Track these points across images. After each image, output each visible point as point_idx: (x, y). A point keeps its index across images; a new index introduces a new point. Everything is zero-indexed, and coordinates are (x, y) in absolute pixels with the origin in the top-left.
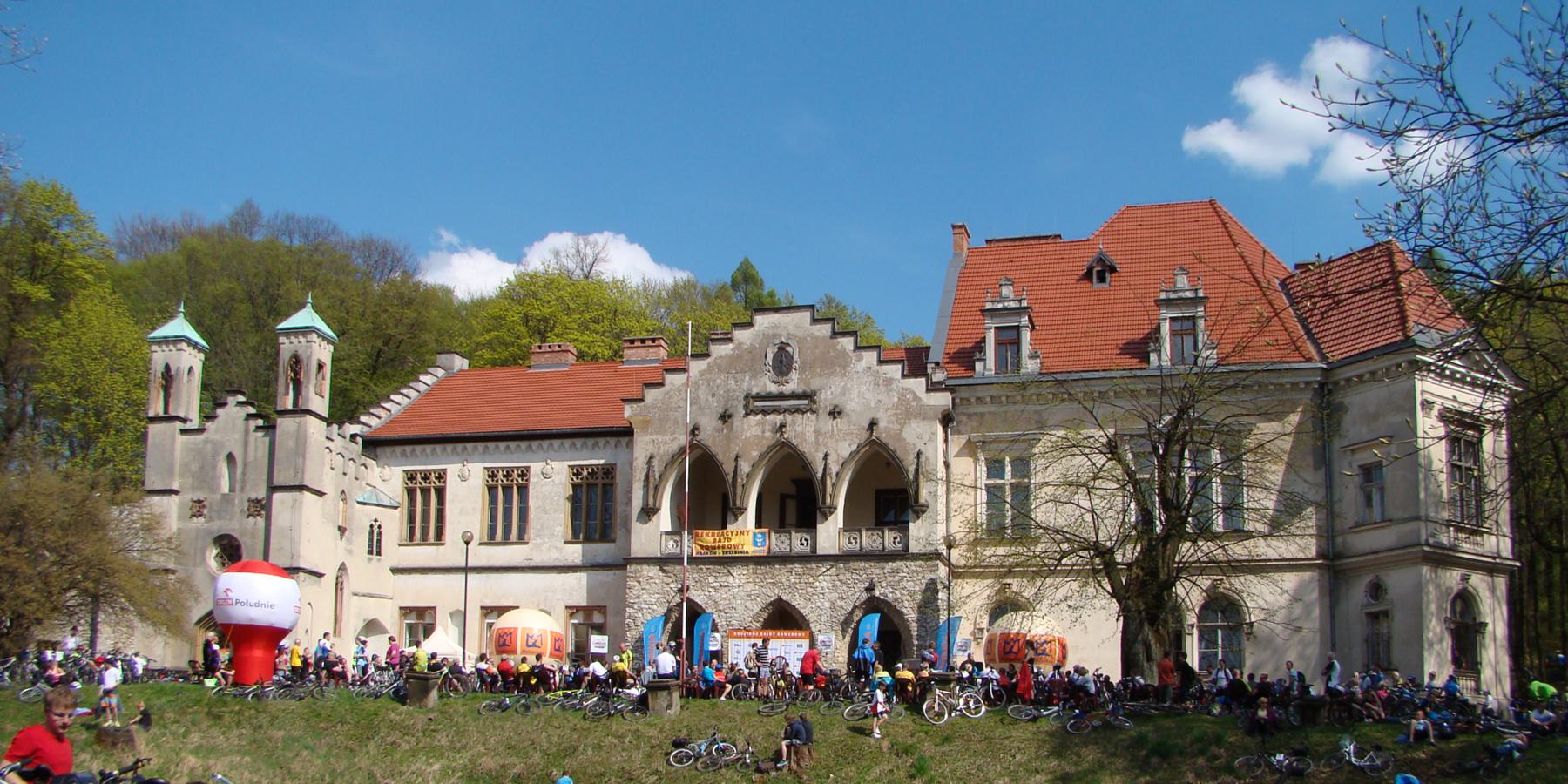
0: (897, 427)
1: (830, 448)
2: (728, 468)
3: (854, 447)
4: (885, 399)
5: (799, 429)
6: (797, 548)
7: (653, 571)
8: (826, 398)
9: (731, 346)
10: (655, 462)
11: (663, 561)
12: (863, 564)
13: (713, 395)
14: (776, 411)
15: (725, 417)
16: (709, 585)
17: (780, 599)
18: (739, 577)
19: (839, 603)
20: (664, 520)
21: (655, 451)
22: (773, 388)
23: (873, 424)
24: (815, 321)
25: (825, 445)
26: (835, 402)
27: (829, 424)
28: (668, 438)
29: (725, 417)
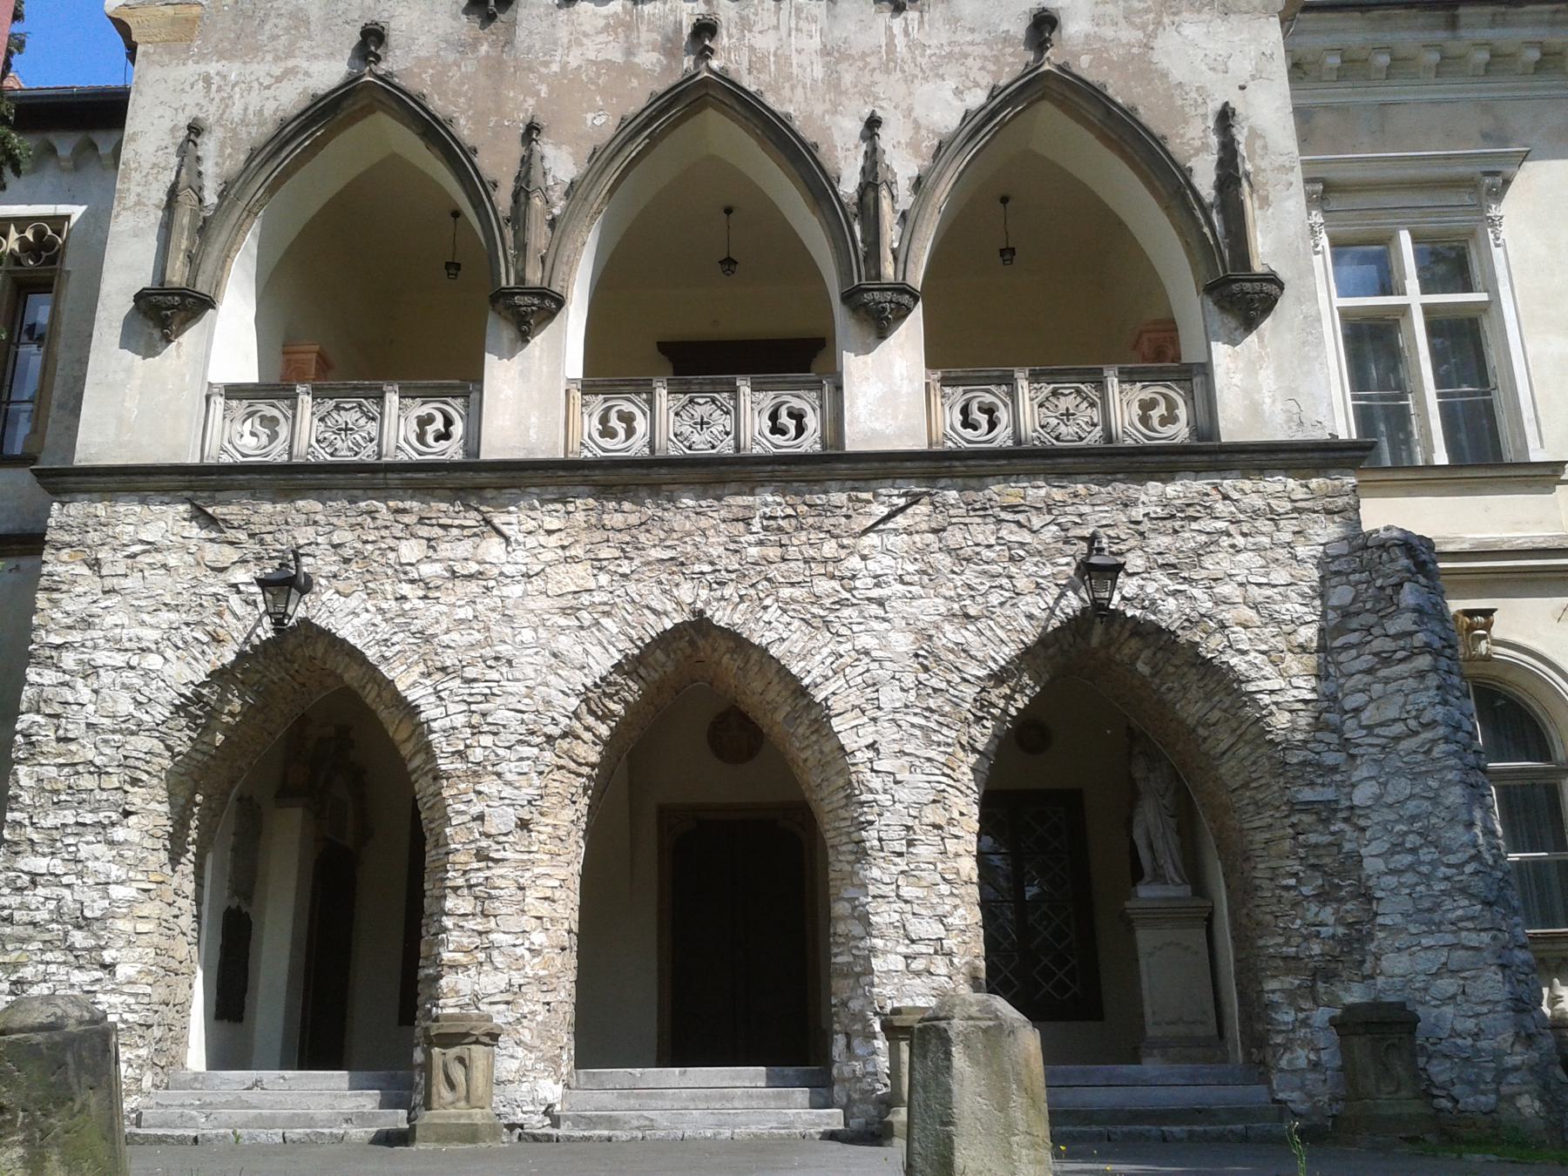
0: (1128, 35)
2: (497, 164)
3: (977, 98)
5: (765, 43)
6: (757, 436)
7: (165, 521)
10: (209, 147)
11: (200, 485)
12: (1038, 492)
16: (402, 571)
17: (700, 625)
18: (531, 533)
19: (952, 634)
20: (231, 340)
21: (210, 114)
23: (1043, 26)
25: (867, 93)
28: (262, 69)
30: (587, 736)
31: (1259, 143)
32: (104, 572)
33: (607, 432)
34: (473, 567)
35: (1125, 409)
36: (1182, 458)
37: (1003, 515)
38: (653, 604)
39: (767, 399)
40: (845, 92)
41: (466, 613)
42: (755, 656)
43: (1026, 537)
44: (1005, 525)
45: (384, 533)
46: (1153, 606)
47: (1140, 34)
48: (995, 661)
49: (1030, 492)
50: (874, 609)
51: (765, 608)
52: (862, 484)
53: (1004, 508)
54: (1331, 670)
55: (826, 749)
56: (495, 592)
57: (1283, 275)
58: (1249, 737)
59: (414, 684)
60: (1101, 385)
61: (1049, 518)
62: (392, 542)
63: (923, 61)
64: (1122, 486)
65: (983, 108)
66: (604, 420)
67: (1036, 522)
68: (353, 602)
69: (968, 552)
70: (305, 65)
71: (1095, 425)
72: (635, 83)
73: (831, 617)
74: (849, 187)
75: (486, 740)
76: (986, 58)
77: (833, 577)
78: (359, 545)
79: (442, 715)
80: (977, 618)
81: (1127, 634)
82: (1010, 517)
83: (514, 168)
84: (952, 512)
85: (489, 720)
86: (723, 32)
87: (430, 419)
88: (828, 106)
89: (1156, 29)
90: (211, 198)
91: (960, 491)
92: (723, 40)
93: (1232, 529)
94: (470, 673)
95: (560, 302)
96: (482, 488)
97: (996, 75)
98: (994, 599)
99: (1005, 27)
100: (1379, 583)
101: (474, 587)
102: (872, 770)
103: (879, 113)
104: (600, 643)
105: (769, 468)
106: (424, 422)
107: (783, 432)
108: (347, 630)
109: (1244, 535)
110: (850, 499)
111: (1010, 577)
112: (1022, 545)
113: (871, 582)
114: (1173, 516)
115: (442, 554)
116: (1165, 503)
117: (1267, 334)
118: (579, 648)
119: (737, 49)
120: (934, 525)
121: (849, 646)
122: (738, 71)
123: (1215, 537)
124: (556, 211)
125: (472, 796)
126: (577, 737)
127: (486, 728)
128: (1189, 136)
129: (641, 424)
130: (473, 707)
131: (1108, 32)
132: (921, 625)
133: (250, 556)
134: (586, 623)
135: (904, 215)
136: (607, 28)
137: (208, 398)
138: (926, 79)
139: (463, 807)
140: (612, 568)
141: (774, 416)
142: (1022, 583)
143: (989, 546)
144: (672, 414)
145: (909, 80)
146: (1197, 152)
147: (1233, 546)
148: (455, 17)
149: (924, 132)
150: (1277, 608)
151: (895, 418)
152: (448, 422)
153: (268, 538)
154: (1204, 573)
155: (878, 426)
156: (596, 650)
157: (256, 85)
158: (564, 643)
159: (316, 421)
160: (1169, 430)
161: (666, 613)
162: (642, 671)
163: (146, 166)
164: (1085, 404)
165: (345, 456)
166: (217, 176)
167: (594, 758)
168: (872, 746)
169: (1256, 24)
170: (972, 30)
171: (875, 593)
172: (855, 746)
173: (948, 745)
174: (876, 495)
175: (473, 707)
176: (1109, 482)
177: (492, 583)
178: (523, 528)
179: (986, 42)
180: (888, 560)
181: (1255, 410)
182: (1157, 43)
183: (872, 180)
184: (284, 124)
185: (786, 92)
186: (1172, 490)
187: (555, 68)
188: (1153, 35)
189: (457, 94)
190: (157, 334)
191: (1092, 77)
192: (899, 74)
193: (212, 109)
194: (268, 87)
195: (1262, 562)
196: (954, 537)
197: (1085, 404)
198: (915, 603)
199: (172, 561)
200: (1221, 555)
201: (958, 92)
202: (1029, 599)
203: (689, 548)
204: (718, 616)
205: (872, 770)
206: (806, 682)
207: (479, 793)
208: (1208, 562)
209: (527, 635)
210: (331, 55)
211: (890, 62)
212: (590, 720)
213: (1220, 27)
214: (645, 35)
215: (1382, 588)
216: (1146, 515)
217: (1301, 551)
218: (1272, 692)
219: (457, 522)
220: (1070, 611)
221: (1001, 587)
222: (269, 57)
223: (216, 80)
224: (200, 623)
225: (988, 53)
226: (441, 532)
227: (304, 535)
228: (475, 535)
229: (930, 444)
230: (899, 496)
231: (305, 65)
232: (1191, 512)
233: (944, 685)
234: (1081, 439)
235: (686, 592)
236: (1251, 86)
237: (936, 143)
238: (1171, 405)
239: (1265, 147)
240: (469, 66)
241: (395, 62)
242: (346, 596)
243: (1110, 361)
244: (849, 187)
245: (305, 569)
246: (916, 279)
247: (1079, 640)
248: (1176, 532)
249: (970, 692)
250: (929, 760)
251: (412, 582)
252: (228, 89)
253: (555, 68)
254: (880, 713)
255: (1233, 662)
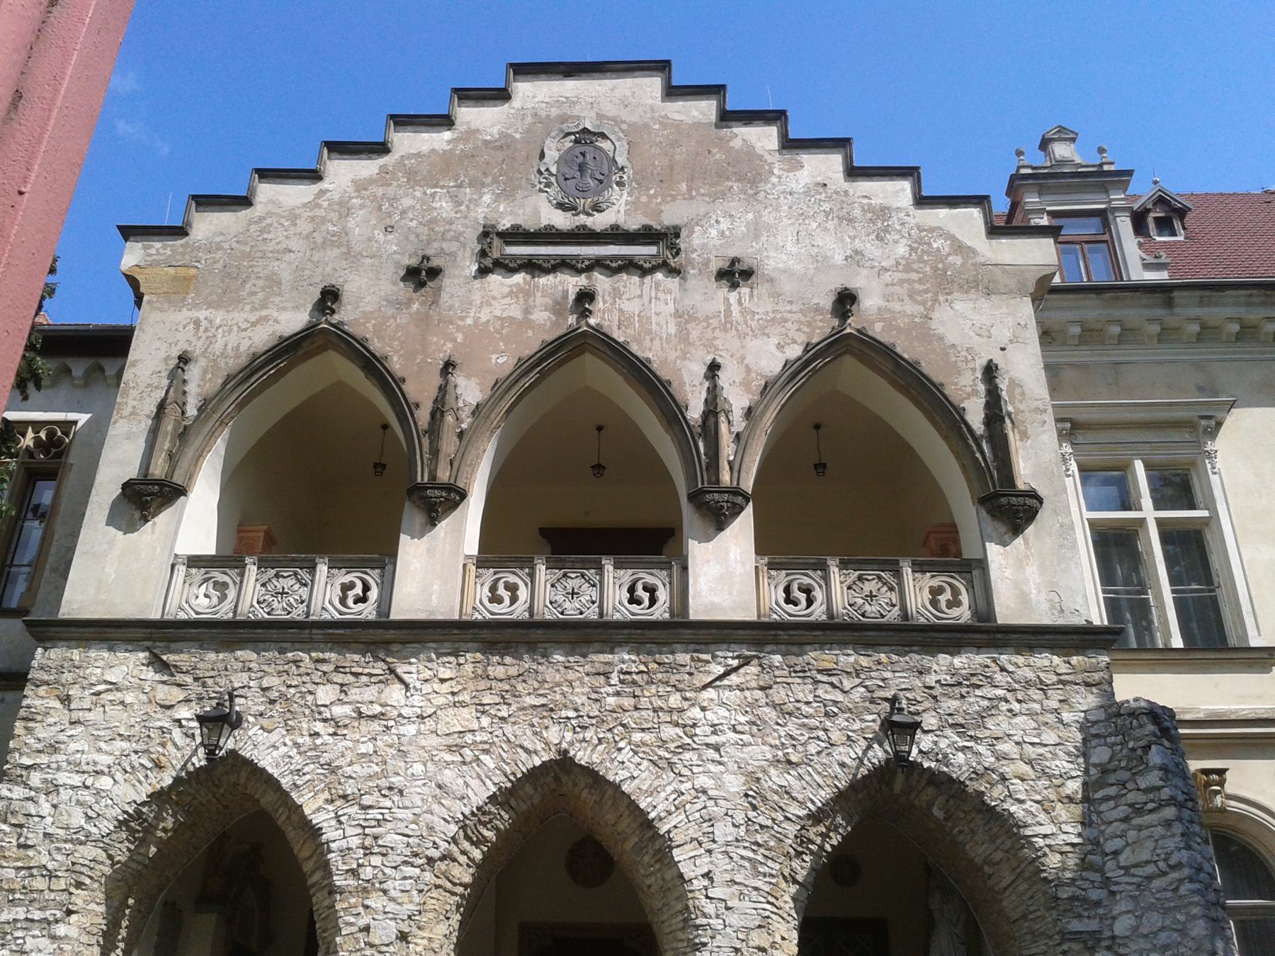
0: (911, 308)
1: (721, 348)
3: (795, 351)
4: (871, 248)
5: (632, 307)
6: (617, 605)
7: (125, 666)
8: (709, 239)
9: (447, 135)
10: (193, 373)
11: (157, 637)
12: (849, 659)
13: (388, 229)
14: (564, 265)
15: (421, 275)
16: (317, 712)
18: (427, 683)
19: (777, 777)
20: (197, 521)
21: (197, 348)
22: (562, 221)
23: (845, 301)
24: (673, 92)
25: (710, 345)
26: (733, 252)
27: (716, 299)
28: (241, 316)
29: (421, 275)
30: (463, 859)
31: (1018, 391)
32: (73, 706)
33: (495, 599)
34: (377, 709)
35: (918, 593)
36: (966, 636)
37: (819, 677)
38: (526, 744)
39: (626, 576)
40: (693, 344)
41: (367, 748)
42: (610, 792)
43: (839, 697)
44: (821, 685)
45: (305, 679)
46: (945, 760)
47: (921, 308)
48: (813, 802)
49: (842, 658)
50: (711, 753)
51: (620, 750)
52: (703, 647)
53: (820, 671)
54: (1094, 818)
55: (668, 876)
56: (394, 731)
57: (1042, 492)
58: (1027, 874)
59: (318, 810)
60: (898, 574)
61: (857, 681)
62: (310, 687)
63: (753, 324)
64: (918, 657)
65: (800, 358)
66: (493, 589)
67: (847, 684)
68: (274, 737)
69: (790, 707)
70: (275, 314)
71: (894, 606)
72: (530, 333)
73: (675, 759)
74: (695, 413)
75: (376, 860)
76: (801, 323)
77: (677, 725)
78: (283, 689)
79: (339, 835)
80: (798, 765)
81: (924, 782)
82: (825, 678)
83: (434, 393)
84: (777, 673)
85: (380, 842)
86: (599, 299)
87: (351, 586)
88: (679, 353)
89: (933, 306)
90: (192, 411)
91: (783, 655)
92: (599, 304)
93: (1009, 696)
94: (367, 800)
95: (463, 495)
96: (388, 643)
97: (810, 335)
98: (813, 748)
99: (816, 301)
100: (1131, 745)
101: (376, 726)
102: (707, 897)
103: (719, 360)
104: (479, 777)
105: (626, 632)
106: (346, 588)
107: (639, 603)
108: (267, 761)
109: (1019, 701)
110: (692, 659)
111: (825, 730)
112: (835, 702)
113: (708, 730)
114: (960, 684)
115: (351, 698)
116: (953, 672)
117: (1031, 538)
118: (460, 781)
119: (610, 311)
120: (762, 683)
121: (689, 785)
122: (610, 327)
123: (995, 702)
124: (464, 426)
125: (361, 909)
126: (454, 860)
127: (376, 850)
128: (961, 384)
129: (523, 593)
130: (367, 831)
131: (896, 306)
132: (750, 768)
133: (193, 697)
134: (468, 759)
135: (738, 435)
136: (510, 294)
137: (173, 566)
138: (755, 336)
139: (352, 919)
140: (493, 712)
141: (632, 590)
142: (836, 736)
143: (808, 703)
144: (549, 586)
145: (742, 336)
146: (969, 396)
147: (1010, 711)
148: (394, 284)
149: (753, 375)
150: (1048, 764)
151: (730, 594)
152: (366, 588)
153: (210, 682)
154: (987, 733)
155: (716, 600)
156: (474, 783)
157: (235, 328)
158: (448, 776)
159: (258, 586)
160: (955, 612)
161: (536, 752)
162: (513, 803)
163: (142, 386)
164: (885, 588)
165: (280, 615)
166: (199, 394)
167: (467, 879)
168: (707, 875)
169: (1013, 302)
170: (791, 302)
171: (713, 740)
172: (692, 875)
173: (772, 876)
174: (714, 657)
175: (367, 831)
176: (906, 654)
177: (391, 723)
178: (421, 676)
179: (801, 311)
180: (723, 712)
181: (1024, 598)
182: (935, 315)
183: (713, 409)
184: (255, 357)
185: (647, 343)
186: (958, 661)
187: (469, 321)
188: (932, 309)
189: (392, 338)
190: (137, 515)
191: (885, 338)
192: (734, 332)
193: (199, 344)
194: (245, 330)
195: (1034, 725)
196: (779, 694)
197: (885, 588)
198: (745, 749)
199: (129, 698)
200: (1000, 718)
201: (780, 347)
202: (841, 749)
203: (558, 697)
204: (580, 754)
205: (707, 897)
206: (652, 815)
207: (367, 907)
208: (990, 723)
209: (418, 768)
210: (296, 308)
211: (727, 323)
212: (466, 845)
213: (984, 304)
214: (539, 299)
215: (1133, 750)
216: (938, 681)
217: (1066, 716)
218: (1045, 836)
219: (366, 671)
220: (876, 761)
221: (818, 738)
222: (248, 308)
223: (204, 323)
224: (147, 751)
225: (802, 319)
226: (352, 679)
227: (239, 679)
228: (380, 682)
229: (759, 616)
230: (733, 658)
231: (275, 314)
232: (974, 680)
233: (769, 823)
234: (883, 616)
235: (553, 734)
236: (1009, 347)
237: (763, 383)
238: (956, 592)
239: (1023, 394)
240: (403, 319)
241: (346, 314)
242: (269, 732)
243: (906, 555)
244: (695, 413)
245: (237, 708)
246: (748, 484)
247: (883, 786)
248: (963, 697)
249: (792, 829)
250: (756, 889)
251: (325, 720)
252: (213, 330)
253: (469, 321)
254: (714, 846)
255: (1013, 809)
